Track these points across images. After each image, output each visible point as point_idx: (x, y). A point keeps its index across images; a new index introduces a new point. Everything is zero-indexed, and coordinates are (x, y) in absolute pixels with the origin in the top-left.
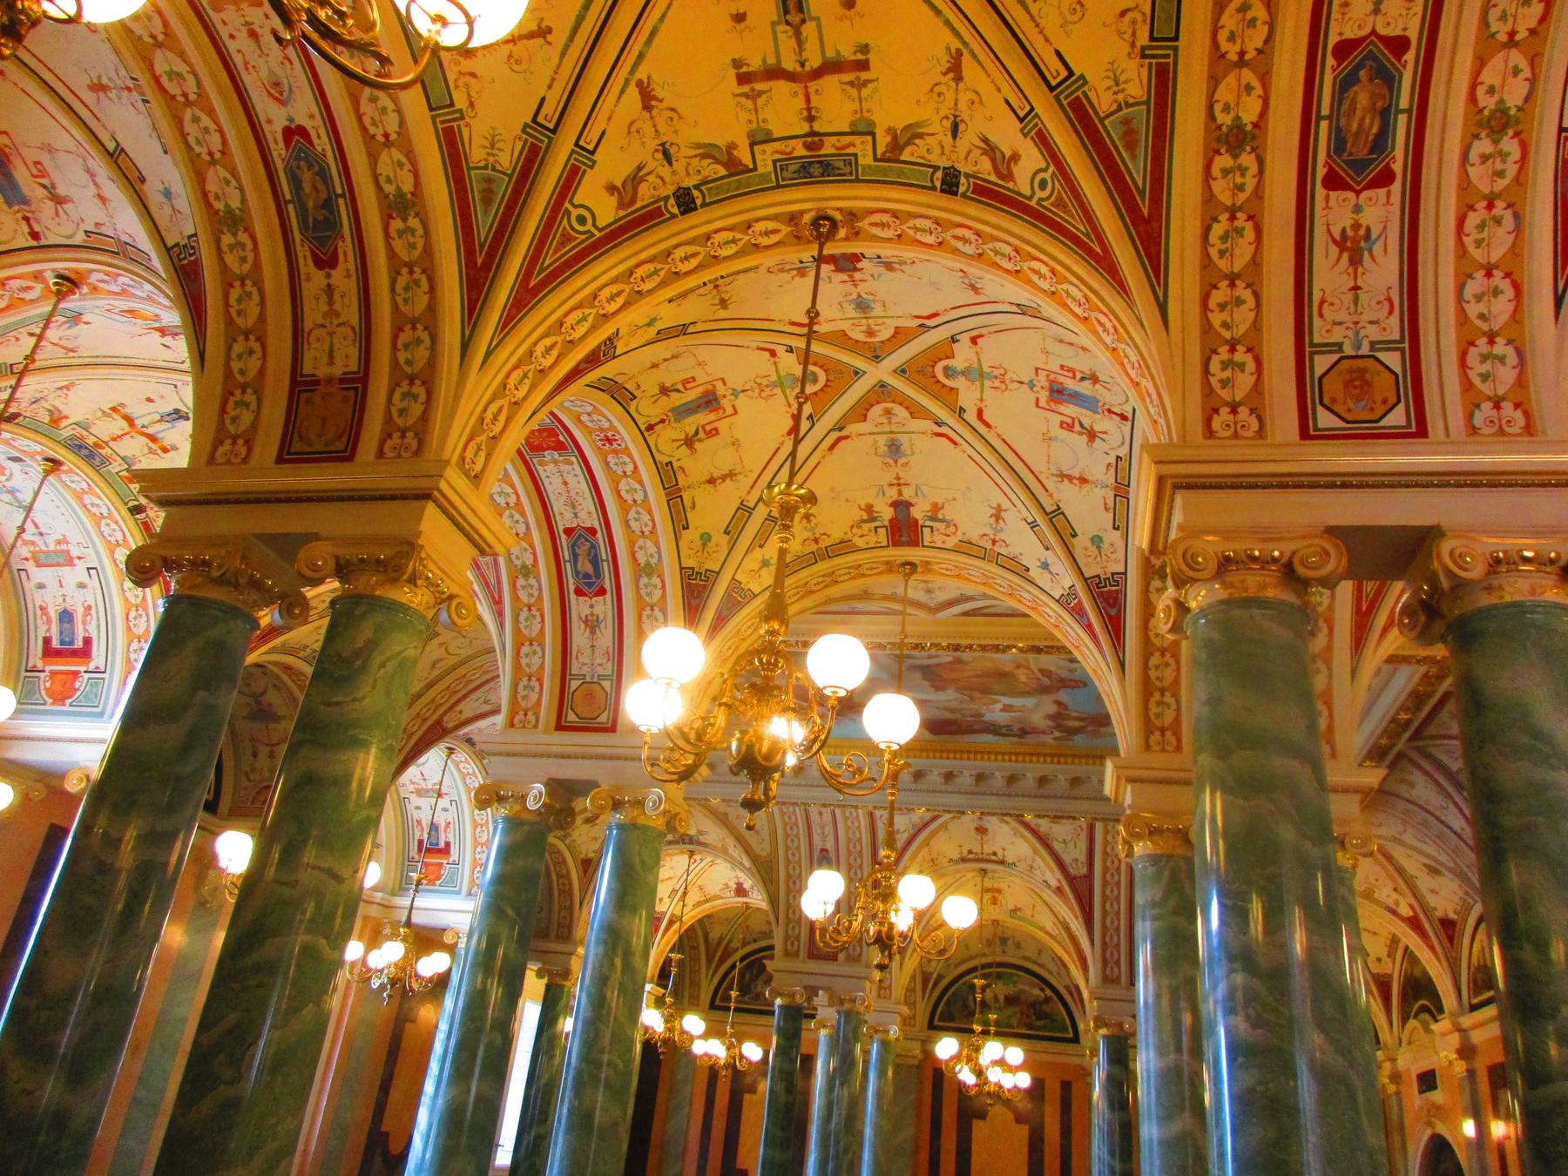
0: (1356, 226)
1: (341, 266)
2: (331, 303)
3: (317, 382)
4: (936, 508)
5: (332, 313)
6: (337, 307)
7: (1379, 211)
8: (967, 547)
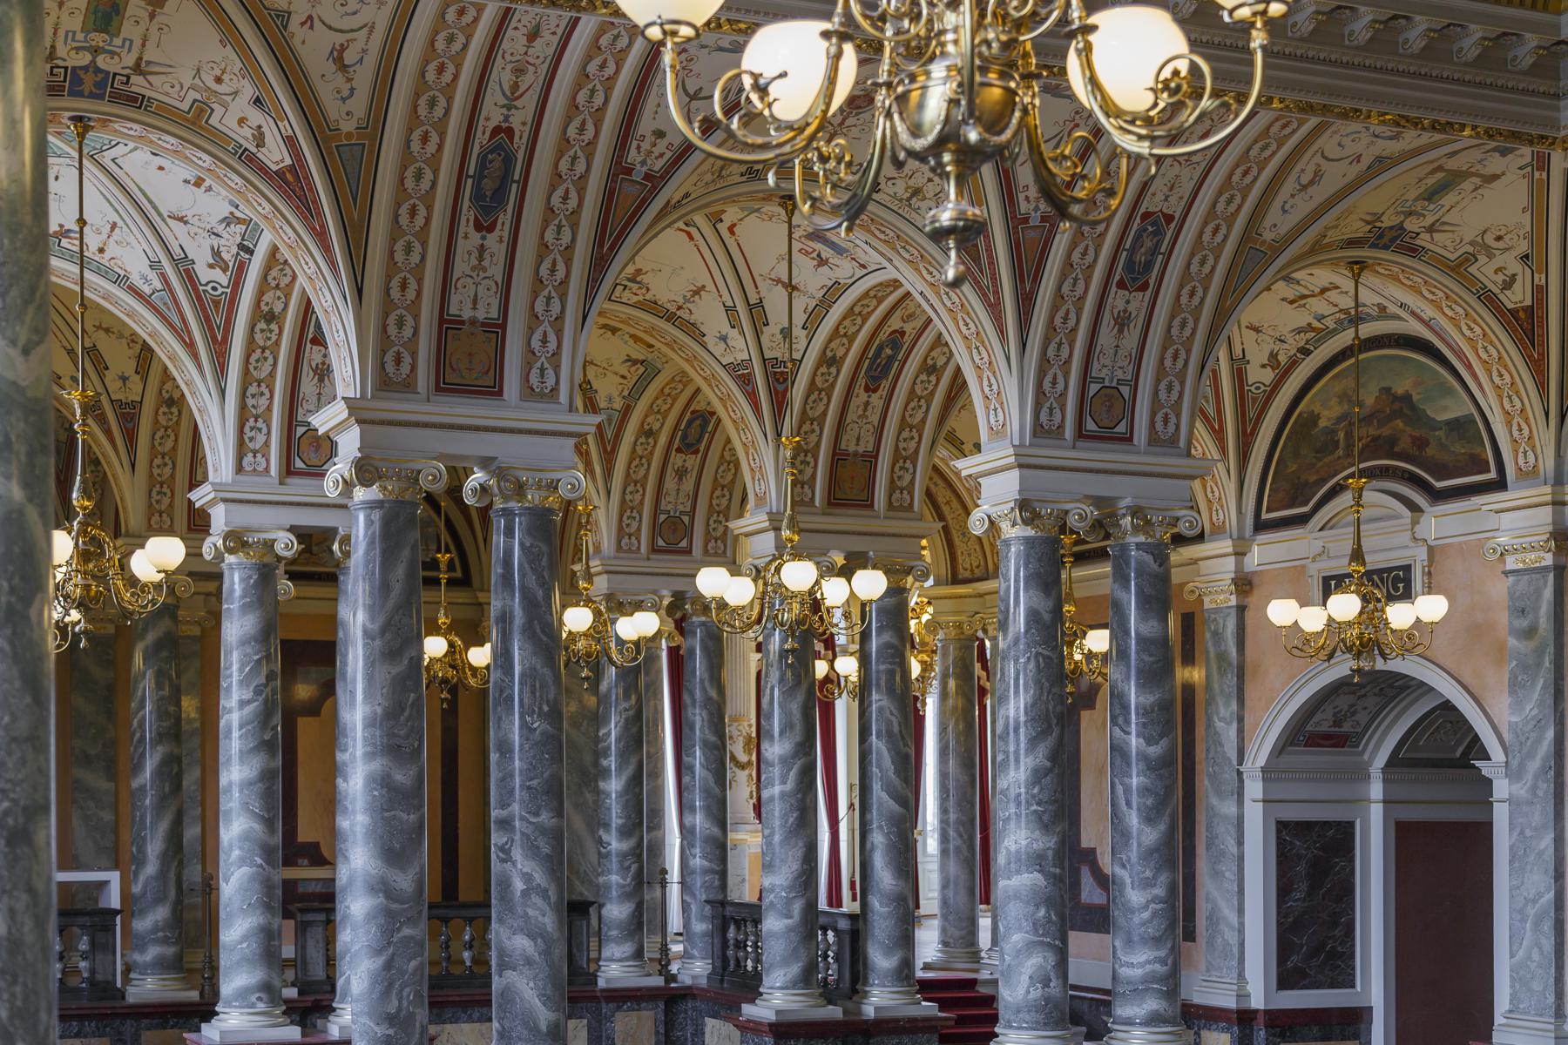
0: (1125, 311)
1: (497, 232)
2: (481, 258)
3: (463, 322)
4: (639, 271)
5: (479, 267)
6: (486, 263)
7: (1137, 303)
8: (652, 307)
